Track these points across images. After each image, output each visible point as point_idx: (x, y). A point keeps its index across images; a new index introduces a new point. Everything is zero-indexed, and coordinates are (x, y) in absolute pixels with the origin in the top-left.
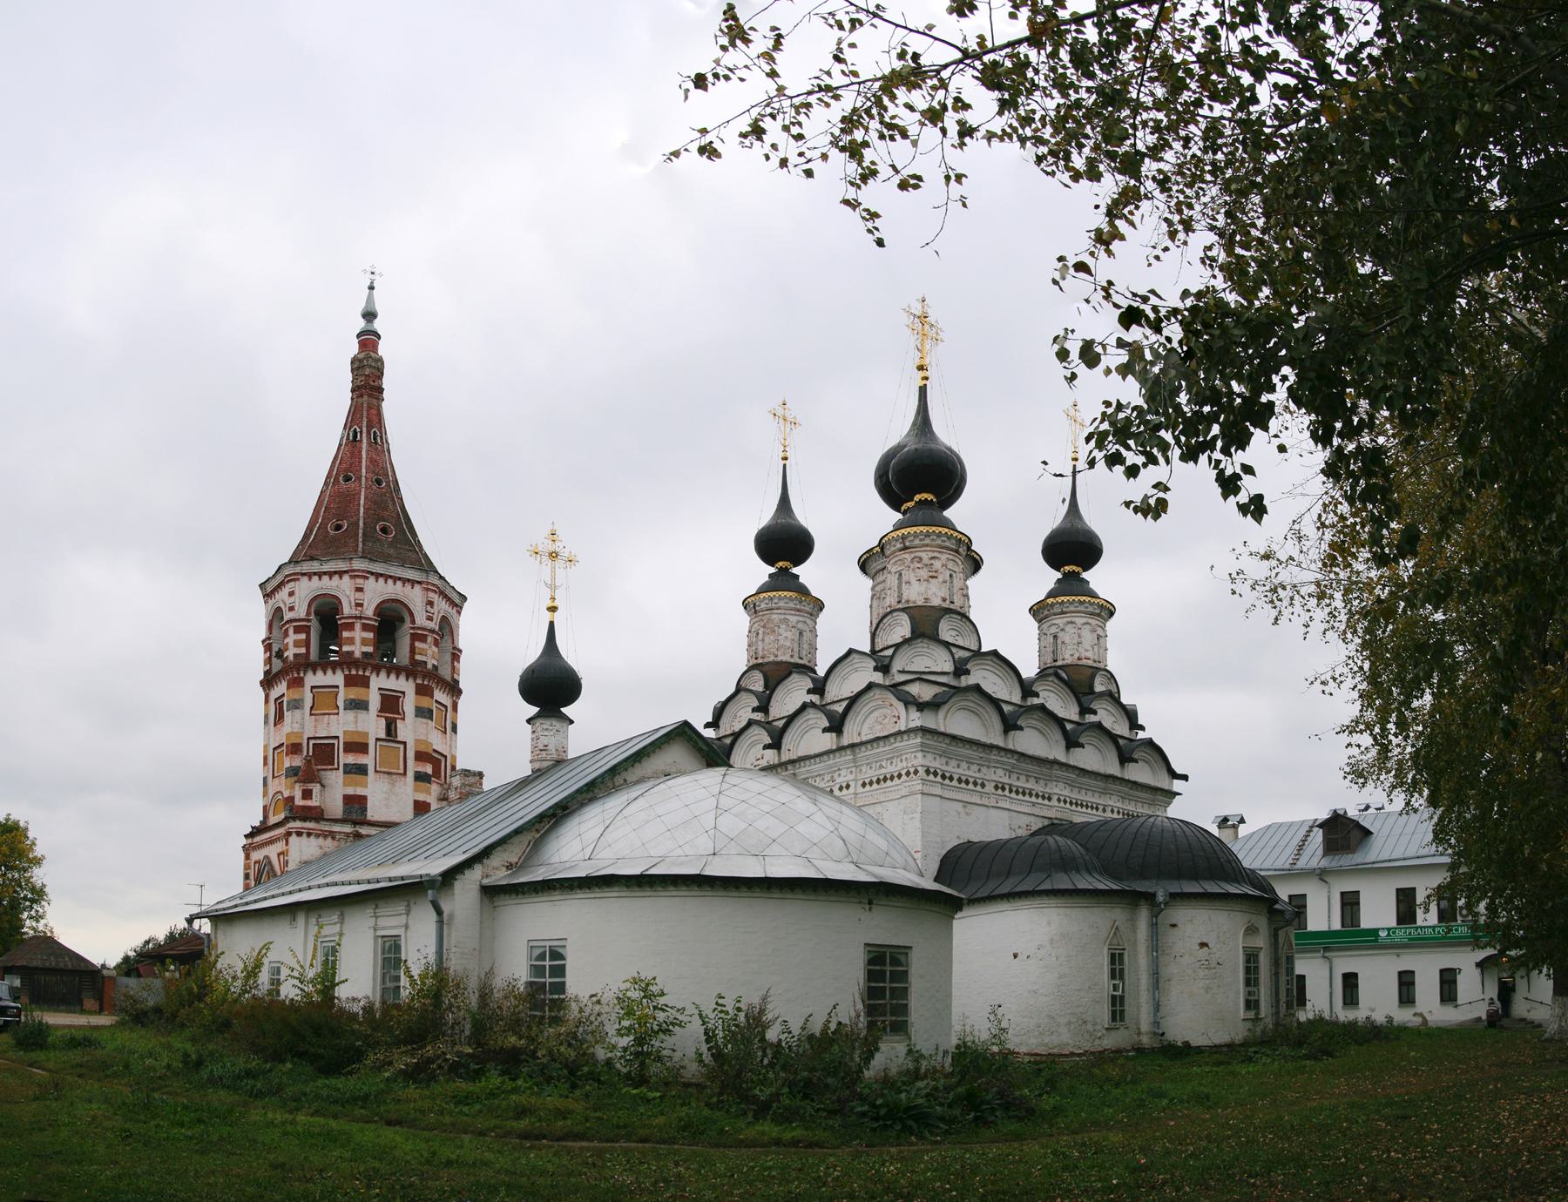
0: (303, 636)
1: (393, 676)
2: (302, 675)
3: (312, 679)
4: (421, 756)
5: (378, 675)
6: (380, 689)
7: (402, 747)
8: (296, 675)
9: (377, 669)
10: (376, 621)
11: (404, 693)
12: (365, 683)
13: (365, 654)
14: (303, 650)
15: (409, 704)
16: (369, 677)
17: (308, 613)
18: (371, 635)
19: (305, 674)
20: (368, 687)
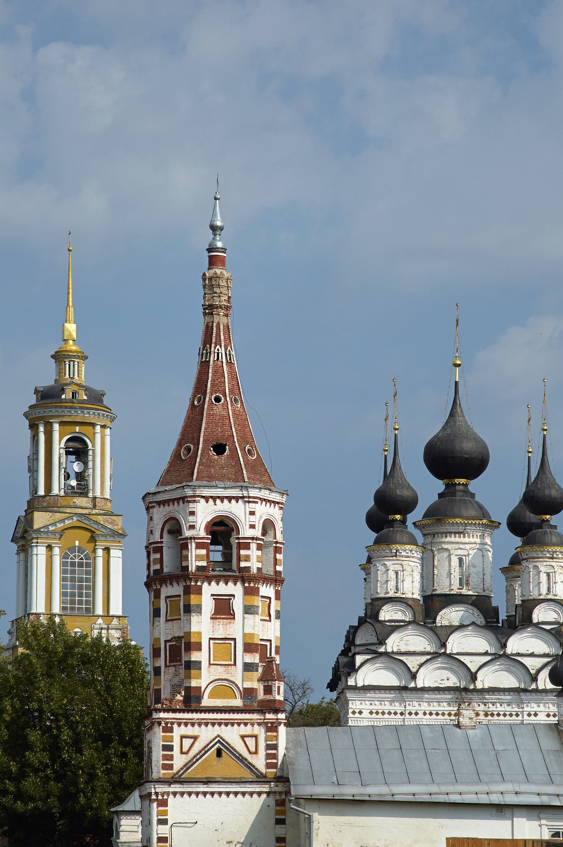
0: (158, 556)
1: (222, 584)
2: (159, 587)
3: (167, 591)
4: (249, 648)
5: (210, 584)
6: (212, 595)
7: (232, 642)
8: (155, 588)
9: (209, 580)
10: (207, 539)
11: (233, 596)
12: (199, 591)
13: (199, 568)
14: (158, 567)
15: (238, 605)
16: (201, 586)
17: (162, 537)
18: (203, 552)
19: (161, 587)
20: (201, 594)
